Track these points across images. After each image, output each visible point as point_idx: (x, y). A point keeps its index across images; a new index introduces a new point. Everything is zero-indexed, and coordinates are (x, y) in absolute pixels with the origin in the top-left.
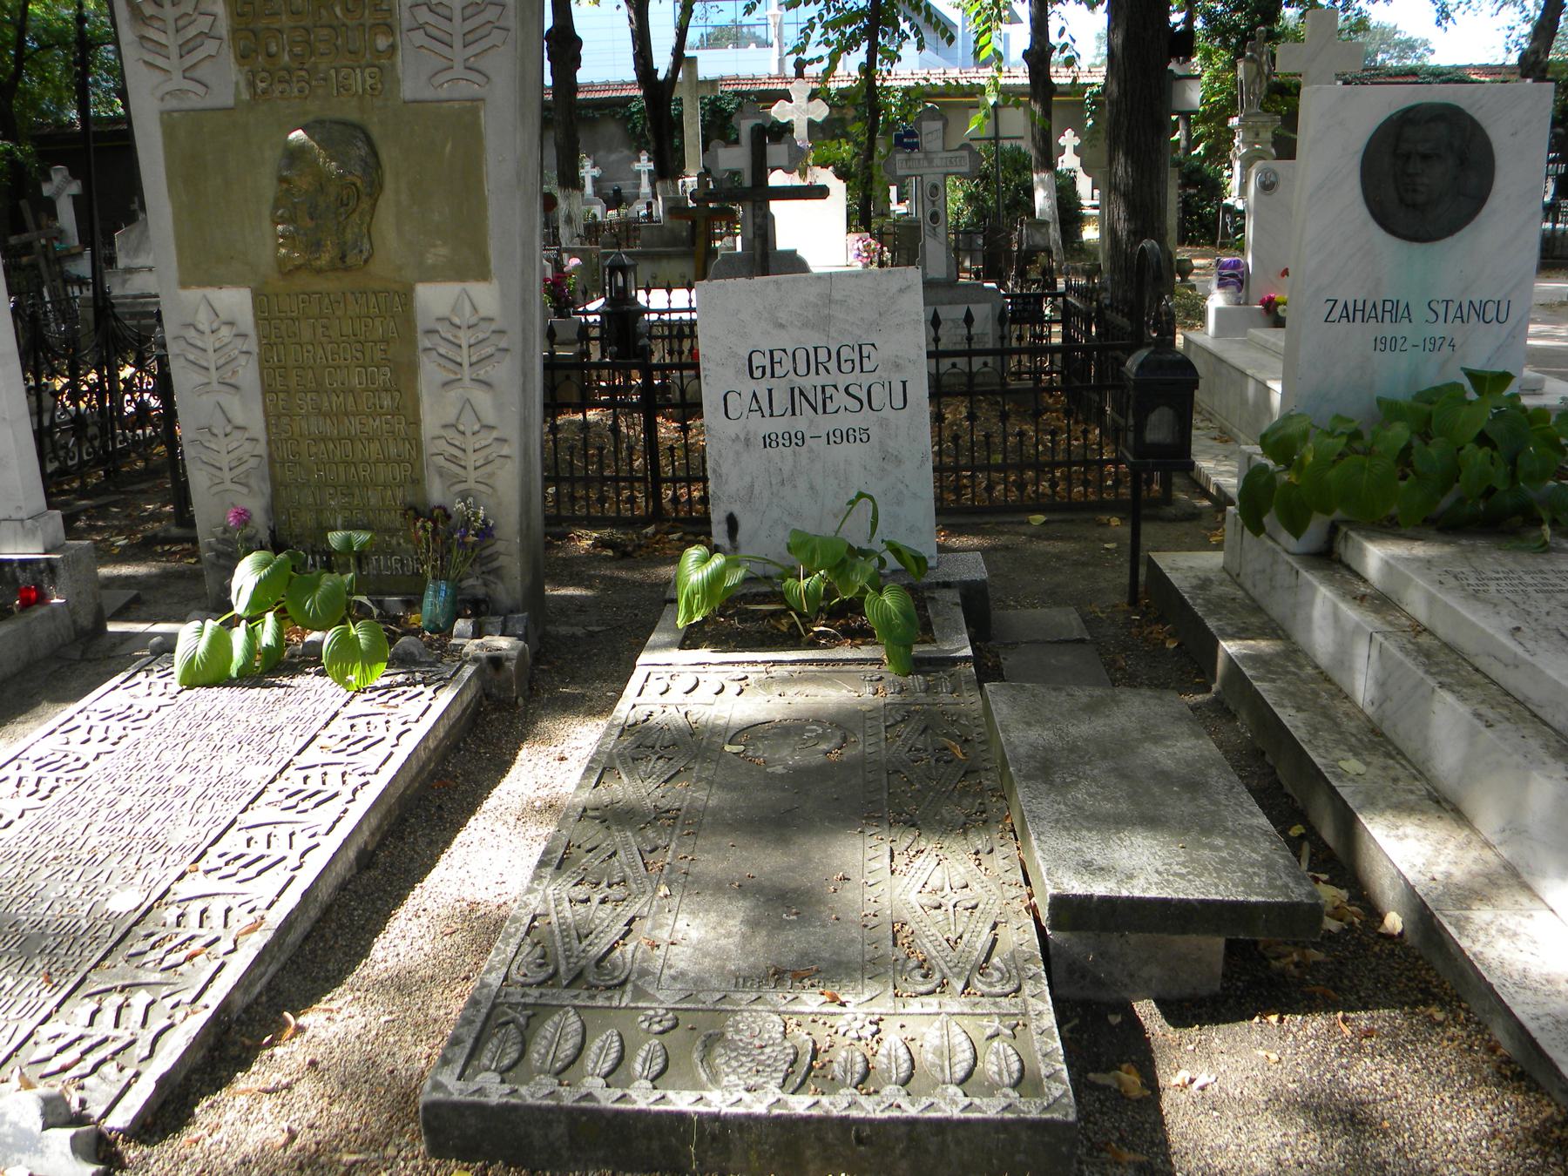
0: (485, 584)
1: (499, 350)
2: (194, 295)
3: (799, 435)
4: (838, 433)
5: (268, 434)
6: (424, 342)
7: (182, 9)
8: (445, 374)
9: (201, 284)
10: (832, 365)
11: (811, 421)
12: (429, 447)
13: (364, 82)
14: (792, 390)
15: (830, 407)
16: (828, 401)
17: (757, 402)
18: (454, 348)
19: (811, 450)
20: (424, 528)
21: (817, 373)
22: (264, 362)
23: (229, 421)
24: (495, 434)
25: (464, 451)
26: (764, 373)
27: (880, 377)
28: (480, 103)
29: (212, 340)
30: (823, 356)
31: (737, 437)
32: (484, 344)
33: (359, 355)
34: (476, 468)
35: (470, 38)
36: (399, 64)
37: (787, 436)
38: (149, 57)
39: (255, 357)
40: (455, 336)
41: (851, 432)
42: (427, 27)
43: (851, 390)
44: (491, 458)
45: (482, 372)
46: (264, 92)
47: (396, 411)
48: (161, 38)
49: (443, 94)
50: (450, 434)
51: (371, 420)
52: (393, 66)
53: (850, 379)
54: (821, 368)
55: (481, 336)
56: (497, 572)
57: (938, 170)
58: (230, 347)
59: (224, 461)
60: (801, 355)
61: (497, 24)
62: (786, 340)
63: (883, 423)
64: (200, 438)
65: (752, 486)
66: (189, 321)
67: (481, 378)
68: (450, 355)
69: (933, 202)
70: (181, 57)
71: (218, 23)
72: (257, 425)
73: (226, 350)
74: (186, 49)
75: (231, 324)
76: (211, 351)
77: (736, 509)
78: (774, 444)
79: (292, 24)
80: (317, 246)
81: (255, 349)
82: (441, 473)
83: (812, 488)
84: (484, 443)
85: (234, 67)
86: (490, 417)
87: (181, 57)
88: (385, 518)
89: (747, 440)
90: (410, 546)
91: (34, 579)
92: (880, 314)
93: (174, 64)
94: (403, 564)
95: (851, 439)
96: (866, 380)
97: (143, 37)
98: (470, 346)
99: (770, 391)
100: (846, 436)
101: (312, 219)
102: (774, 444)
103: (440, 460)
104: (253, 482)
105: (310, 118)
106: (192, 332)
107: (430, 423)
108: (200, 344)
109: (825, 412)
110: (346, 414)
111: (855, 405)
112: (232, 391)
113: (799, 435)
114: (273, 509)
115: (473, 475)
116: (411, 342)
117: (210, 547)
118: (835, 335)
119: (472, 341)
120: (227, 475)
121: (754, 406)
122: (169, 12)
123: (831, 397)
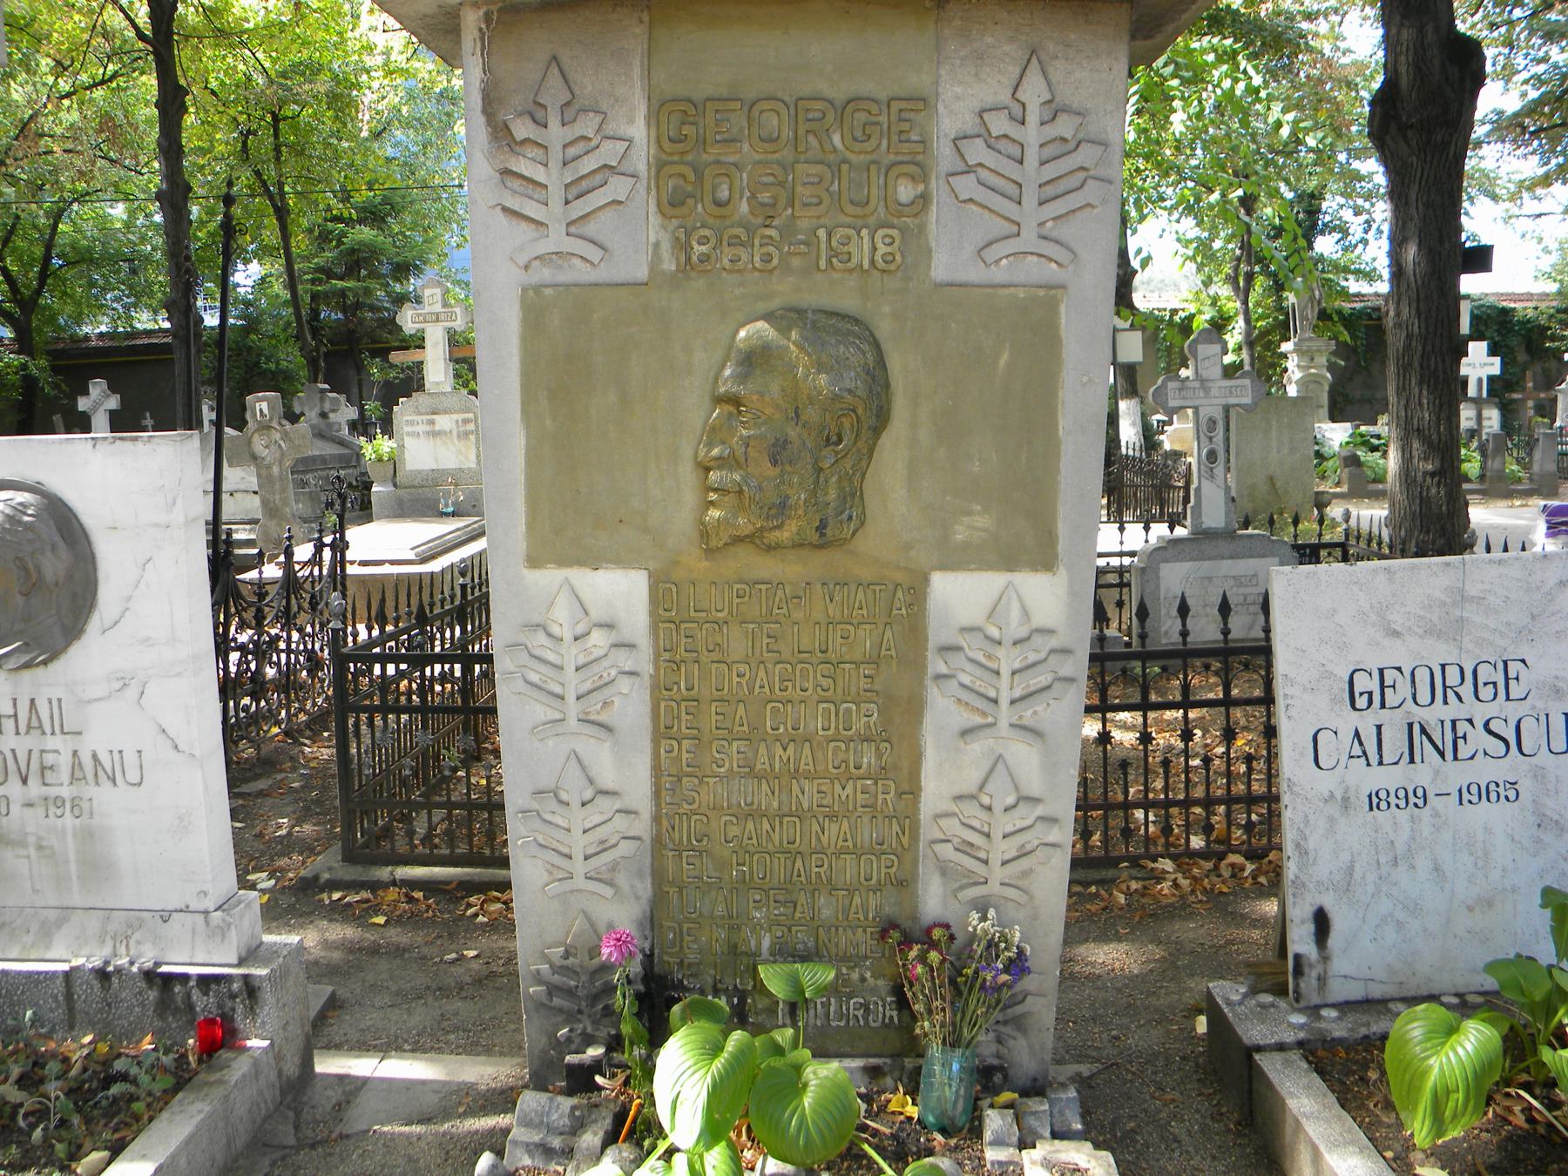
0: (999, 1041)
1: (1059, 679)
2: (549, 578)
3: (1420, 793)
4: (1474, 789)
5: (658, 805)
6: (937, 665)
7: (579, 129)
8: (966, 715)
9: (563, 562)
10: (1467, 690)
11: (1437, 772)
12: (928, 831)
13: (875, 249)
14: (1410, 726)
15: (1464, 751)
16: (1460, 742)
17: (1361, 744)
18: (988, 676)
19: (1436, 814)
20: (922, 959)
21: (1446, 702)
22: (660, 690)
23: (591, 781)
24: (1040, 810)
25: (988, 835)
27: (1534, 708)
28: (1060, 292)
29: (574, 651)
30: (1453, 677)
31: (1332, 795)
32: (1039, 669)
33: (826, 682)
34: (1004, 863)
35: (1050, 191)
36: (932, 227)
37: (1401, 793)
38: (513, 203)
39: (647, 681)
40: (989, 657)
41: (1492, 787)
42: (980, 170)
43: (1493, 726)
44: (1028, 847)
45: (1029, 712)
46: (704, 258)
47: (881, 773)
48: (539, 174)
49: (999, 274)
50: (971, 811)
51: (837, 787)
52: (922, 228)
53: (1490, 710)
54: (1450, 693)
55: (1032, 657)
56: (1019, 1023)
57: (1216, 401)
58: (605, 663)
59: (579, 844)
60: (1423, 677)
61: (1092, 173)
62: (1399, 654)
63: (1539, 774)
64: (536, 806)
65: (1350, 869)
66: (536, 619)
67: (1025, 722)
68: (978, 685)
69: (1211, 439)
70: (567, 203)
71: (633, 152)
72: (637, 786)
73: (595, 668)
74: (574, 191)
75: (609, 626)
76: (570, 668)
77: (1328, 902)
78: (1383, 805)
79: (757, 157)
80: (781, 509)
81: (647, 668)
82: (944, 870)
83: (1437, 869)
85: (655, 220)
86: (1033, 783)
87: (567, 203)
88: (843, 939)
89: (1346, 799)
90: (881, 982)
91: (220, 1006)
92: (1533, 617)
93: (553, 211)
94: (867, 1010)
95: (1493, 796)
96: (1513, 711)
98: (1014, 673)
99: (1379, 727)
100: (1485, 793)
101: (775, 463)
102: (1383, 805)
103: (946, 851)
104: (622, 879)
105: (775, 304)
106: (541, 638)
107: (935, 790)
108: (551, 657)
109: (1456, 758)
110: (796, 775)
111: (1497, 747)
112: (602, 733)
113: (1420, 793)
114: (652, 921)
115: (998, 874)
116: (913, 661)
117: (538, 978)
118: (1470, 646)
119: (1017, 665)
120: (579, 867)
121: (1357, 750)
122: (556, 133)
123: (1464, 737)
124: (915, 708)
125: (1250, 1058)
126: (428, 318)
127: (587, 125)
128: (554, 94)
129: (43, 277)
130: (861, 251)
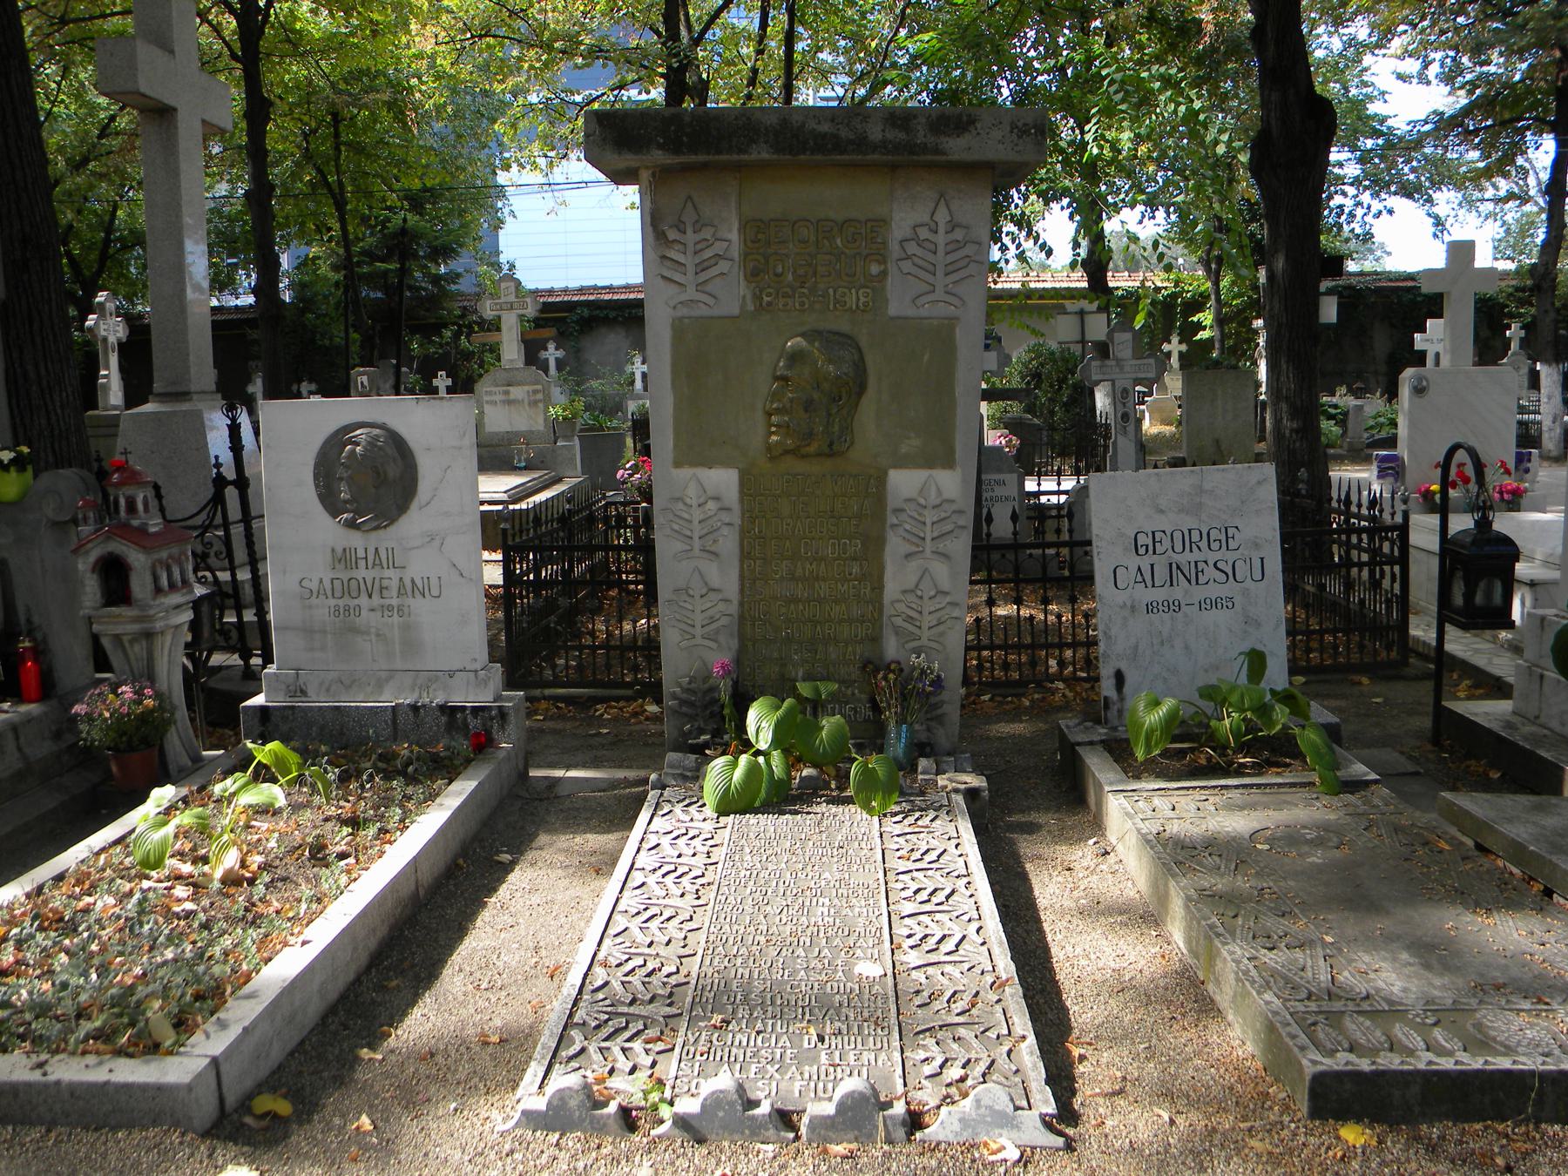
0: (929, 730)
2: (686, 473)
4: (1208, 601)
7: (703, 235)
10: (1204, 544)
11: (1186, 592)
12: (888, 610)
13: (858, 299)
14: (1171, 564)
19: (1186, 615)
20: (885, 678)
22: (744, 533)
23: (706, 584)
24: (948, 599)
26: (1147, 551)
35: (950, 268)
36: (889, 287)
37: (1166, 604)
39: (737, 528)
40: (920, 514)
43: (1219, 565)
46: (769, 304)
48: (681, 258)
49: (924, 312)
50: (911, 598)
53: (1218, 556)
54: (1194, 546)
55: (943, 515)
56: (940, 719)
57: (1128, 376)
59: (699, 619)
60: (1178, 535)
62: (1164, 523)
63: (1246, 593)
65: (1136, 647)
72: (731, 587)
75: (717, 499)
76: (696, 522)
77: (1123, 666)
78: (1155, 610)
80: (809, 436)
81: (738, 521)
82: (897, 631)
83: (1187, 647)
84: (938, 606)
86: (945, 584)
91: (484, 725)
93: (689, 279)
94: (856, 712)
95: (1219, 605)
96: (1231, 556)
97: (664, 257)
99: (1152, 565)
100: (1215, 604)
101: (806, 411)
102: (1155, 610)
103: (899, 621)
104: (722, 639)
106: (680, 505)
107: (891, 589)
108: (686, 516)
110: (817, 578)
112: (712, 557)
114: (738, 661)
115: (926, 634)
117: (674, 696)
119: (935, 519)
120: (698, 631)
121: (1139, 579)
122: (690, 237)
124: (880, 542)
125: (1074, 749)
126: (504, 307)
127: (707, 233)
128: (689, 216)
129: (104, 257)
130: (851, 300)
